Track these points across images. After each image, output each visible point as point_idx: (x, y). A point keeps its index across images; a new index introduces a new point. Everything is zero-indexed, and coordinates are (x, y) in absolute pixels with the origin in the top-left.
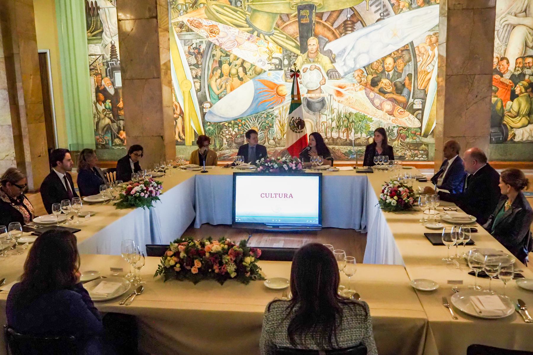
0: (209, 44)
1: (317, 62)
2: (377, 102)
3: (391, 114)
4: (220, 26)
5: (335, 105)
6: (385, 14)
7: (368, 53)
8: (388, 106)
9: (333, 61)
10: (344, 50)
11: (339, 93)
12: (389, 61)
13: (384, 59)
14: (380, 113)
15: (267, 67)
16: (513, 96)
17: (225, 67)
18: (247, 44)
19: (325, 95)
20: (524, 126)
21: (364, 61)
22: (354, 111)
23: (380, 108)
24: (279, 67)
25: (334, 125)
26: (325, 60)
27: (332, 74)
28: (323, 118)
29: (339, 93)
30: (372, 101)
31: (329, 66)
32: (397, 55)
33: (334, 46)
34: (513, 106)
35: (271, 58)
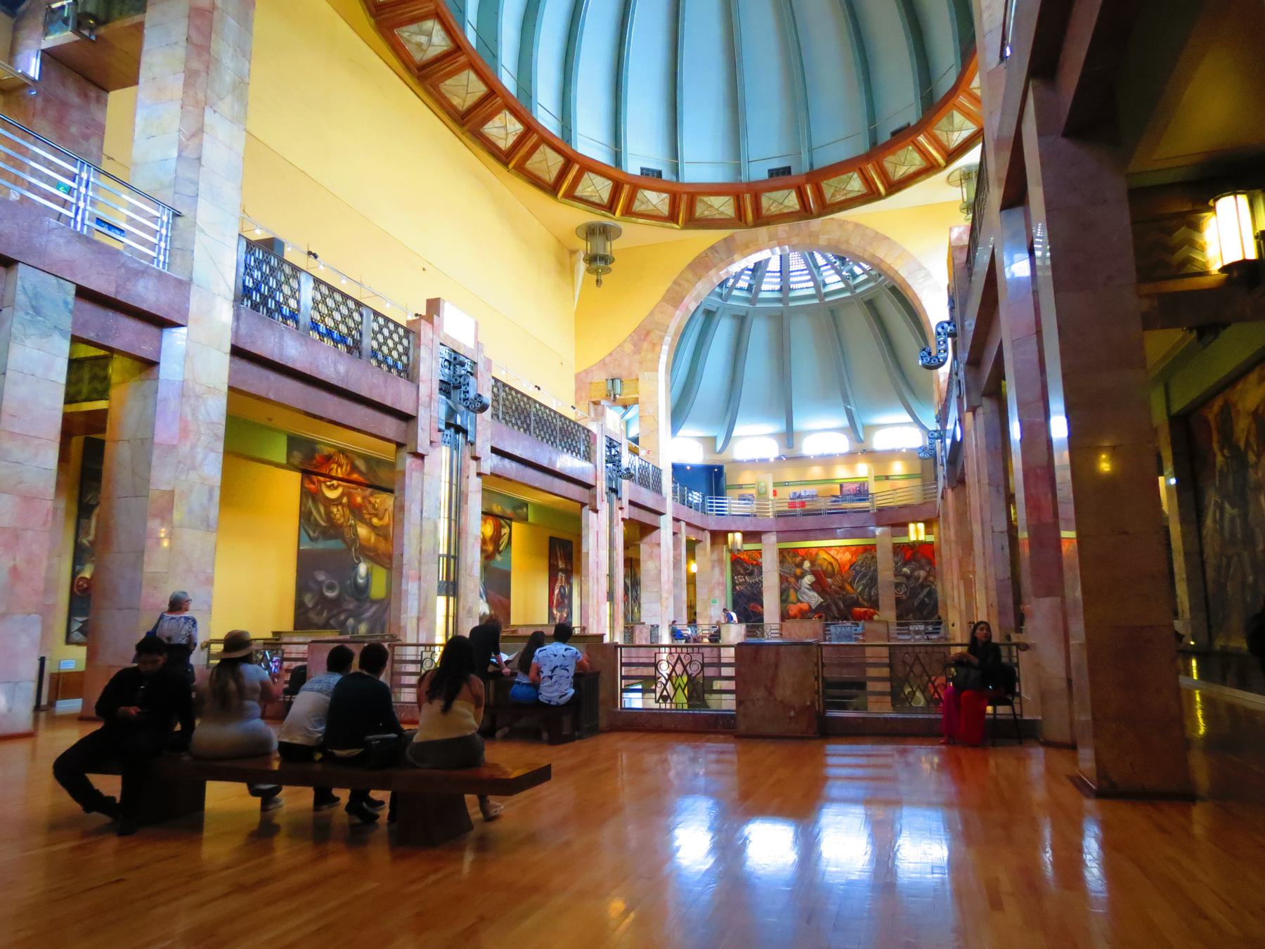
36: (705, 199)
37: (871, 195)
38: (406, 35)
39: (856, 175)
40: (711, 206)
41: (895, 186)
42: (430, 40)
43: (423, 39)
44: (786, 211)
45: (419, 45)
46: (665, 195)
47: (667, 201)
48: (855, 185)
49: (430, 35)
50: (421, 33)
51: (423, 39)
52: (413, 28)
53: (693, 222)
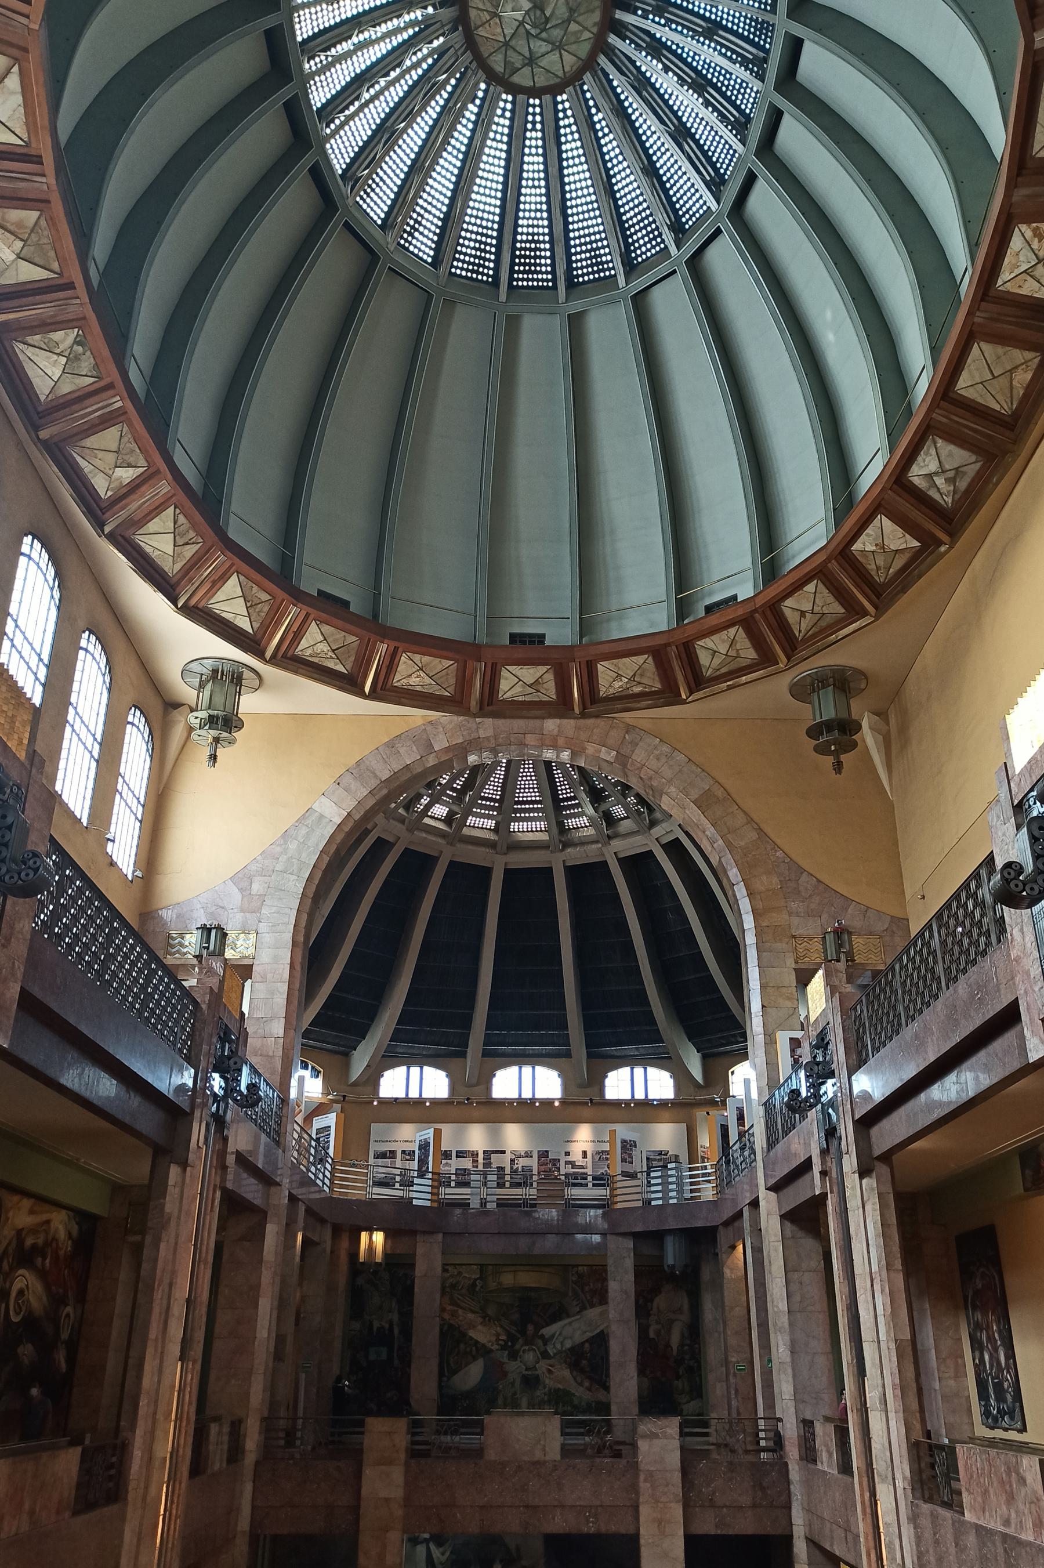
0: (451, 1326)
1: (532, 1345)
2: (579, 1379)
3: (589, 1389)
4: (460, 1311)
5: (547, 1381)
6: (583, 1308)
7: (571, 1338)
8: (587, 1384)
9: (545, 1344)
10: (553, 1336)
11: (550, 1372)
12: (587, 1345)
13: (583, 1343)
14: (581, 1389)
15: (495, 1347)
16: (678, 1377)
17: (462, 1346)
18: (480, 1327)
19: (539, 1372)
20: (688, 1402)
21: (568, 1344)
22: (561, 1387)
23: (581, 1384)
24: (504, 1348)
25: (546, 1398)
26: (540, 1342)
27: (545, 1355)
28: (538, 1393)
29: (550, 1372)
30: (575, 1379)
31: (542, 1349)
32: (591, 1340)
33: (547, 1331)
34: (679, 1384)
35: (498, 1340)
38: (949, 500)
42: (936, 473)
43: (939, 481)
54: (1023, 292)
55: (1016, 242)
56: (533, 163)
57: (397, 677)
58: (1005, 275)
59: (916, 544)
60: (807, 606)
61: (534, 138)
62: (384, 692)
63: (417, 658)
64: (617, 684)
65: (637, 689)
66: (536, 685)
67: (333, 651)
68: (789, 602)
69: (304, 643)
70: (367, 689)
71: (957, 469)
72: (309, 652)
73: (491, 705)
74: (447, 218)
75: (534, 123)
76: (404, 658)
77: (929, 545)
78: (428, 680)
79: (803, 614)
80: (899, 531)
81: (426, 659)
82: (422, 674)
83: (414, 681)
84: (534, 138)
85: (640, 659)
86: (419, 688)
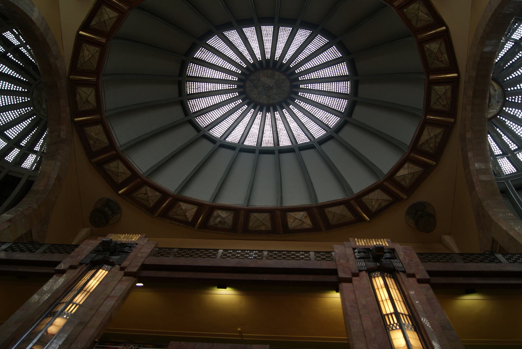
36: (420, 143)
37: (446, 37)
38: (212, 223)
39: (427, 46)
40: (427, 141)
41: (439, 21)
42: (221, 217)
44: (449, 94)
45: (220, 222)
46: (406, 165)
47: (411, 165)
48: (434, 46)
49: (219, 216)
50: (216, 218)
51: (219, 219)
52: (212, 219)
53: (437, 154)
54: (289, 220)
55: (302, 213)
56: (219, 87)
57: (88, 46)
58: (292, 214)
59: (190, 220)
60: (150, 194)
61: (226, 87)
62: (80, 41)
63: (98, 54)
64: (93, 134)
65: (91, 142)
66: (87, 102)
67: (104, 21)
68: (148, 188)
69: (108, 10)
70: (81, 32)
71: (225, 222)
72: (104, 11)
73: (73, 85)
74: (204, 62)
75: (230, 87)
76: (97, 49)
77: (192, 224)
78: (87, 59)
79: (146, 194)
80: (193, 214)
81: (97, 58)
82: (90, 56)
83: (86, 53)
84: (226, 87)
85: (106, 141)
86: (81, 54)
